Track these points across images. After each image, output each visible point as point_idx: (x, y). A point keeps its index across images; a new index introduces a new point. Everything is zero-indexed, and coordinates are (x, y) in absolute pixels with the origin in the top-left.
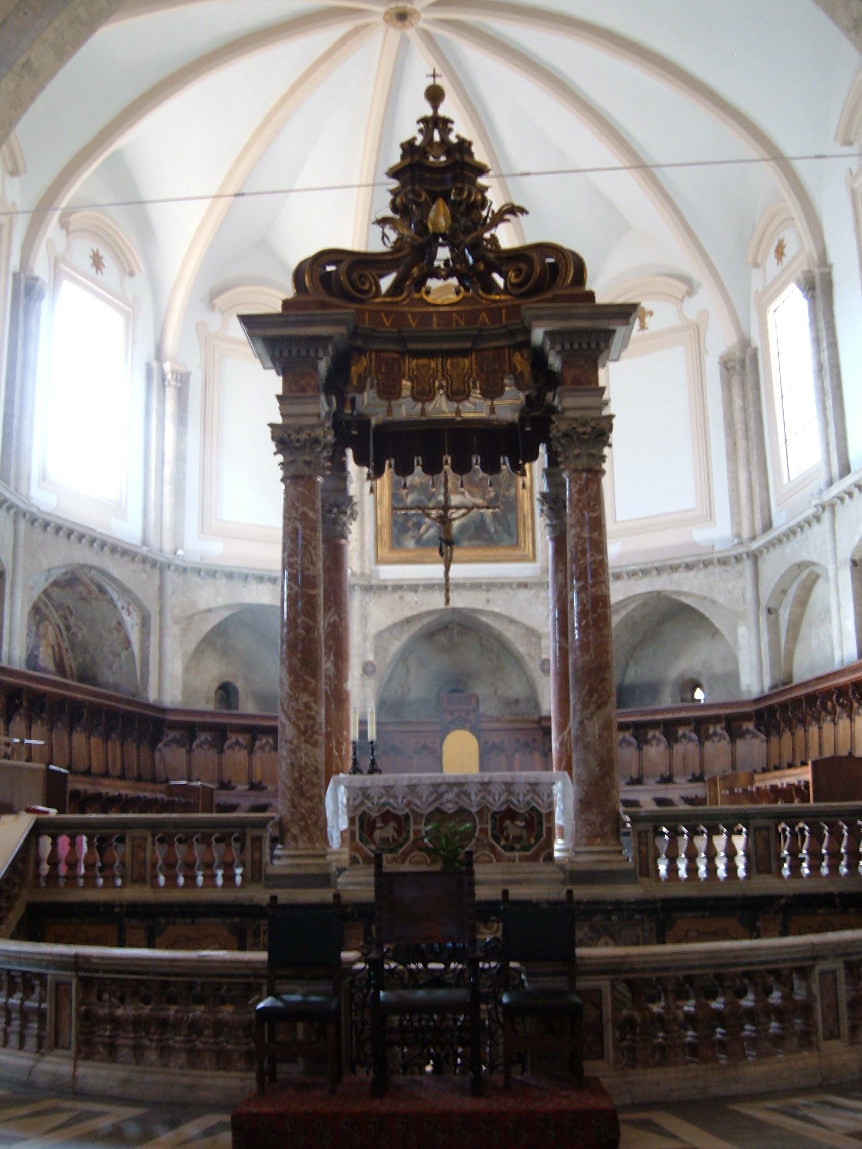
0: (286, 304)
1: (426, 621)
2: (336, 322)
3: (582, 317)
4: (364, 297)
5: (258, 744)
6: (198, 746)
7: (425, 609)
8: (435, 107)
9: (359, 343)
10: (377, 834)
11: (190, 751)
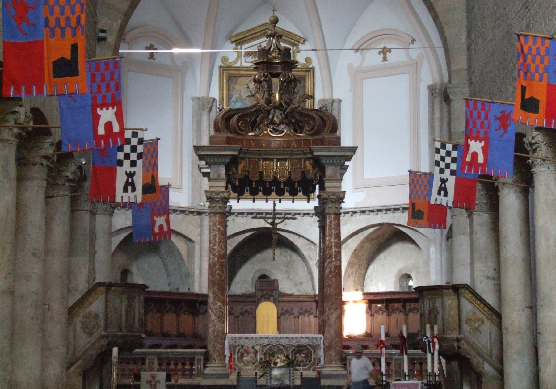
2: (234, 150)
3: (335, 151)
4: (243, 133)
5: (149, 309)
7: (247, 227)
9: (242, 155)
10: (244, 359)
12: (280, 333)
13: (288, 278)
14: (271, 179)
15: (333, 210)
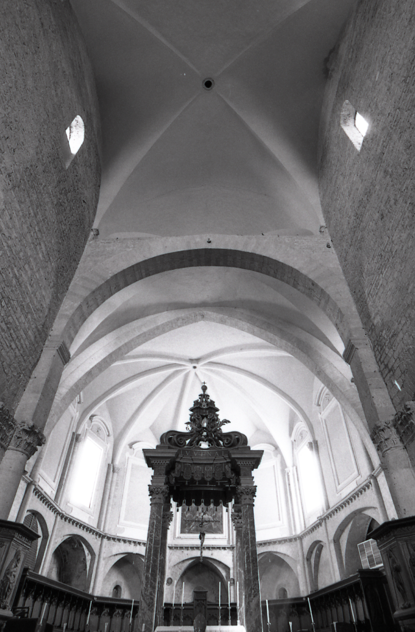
0: (157, 447)
1: (190, 561)
2: (172, 453)
4: (181, 446)
5: (126, 614)
6: (104, 615)
7: (189, 557)
8: (204, 392)
11: (99, 617)
12: (165, 604)
13: (214, 593)
14: (200, 479)
15: (247, 501)
